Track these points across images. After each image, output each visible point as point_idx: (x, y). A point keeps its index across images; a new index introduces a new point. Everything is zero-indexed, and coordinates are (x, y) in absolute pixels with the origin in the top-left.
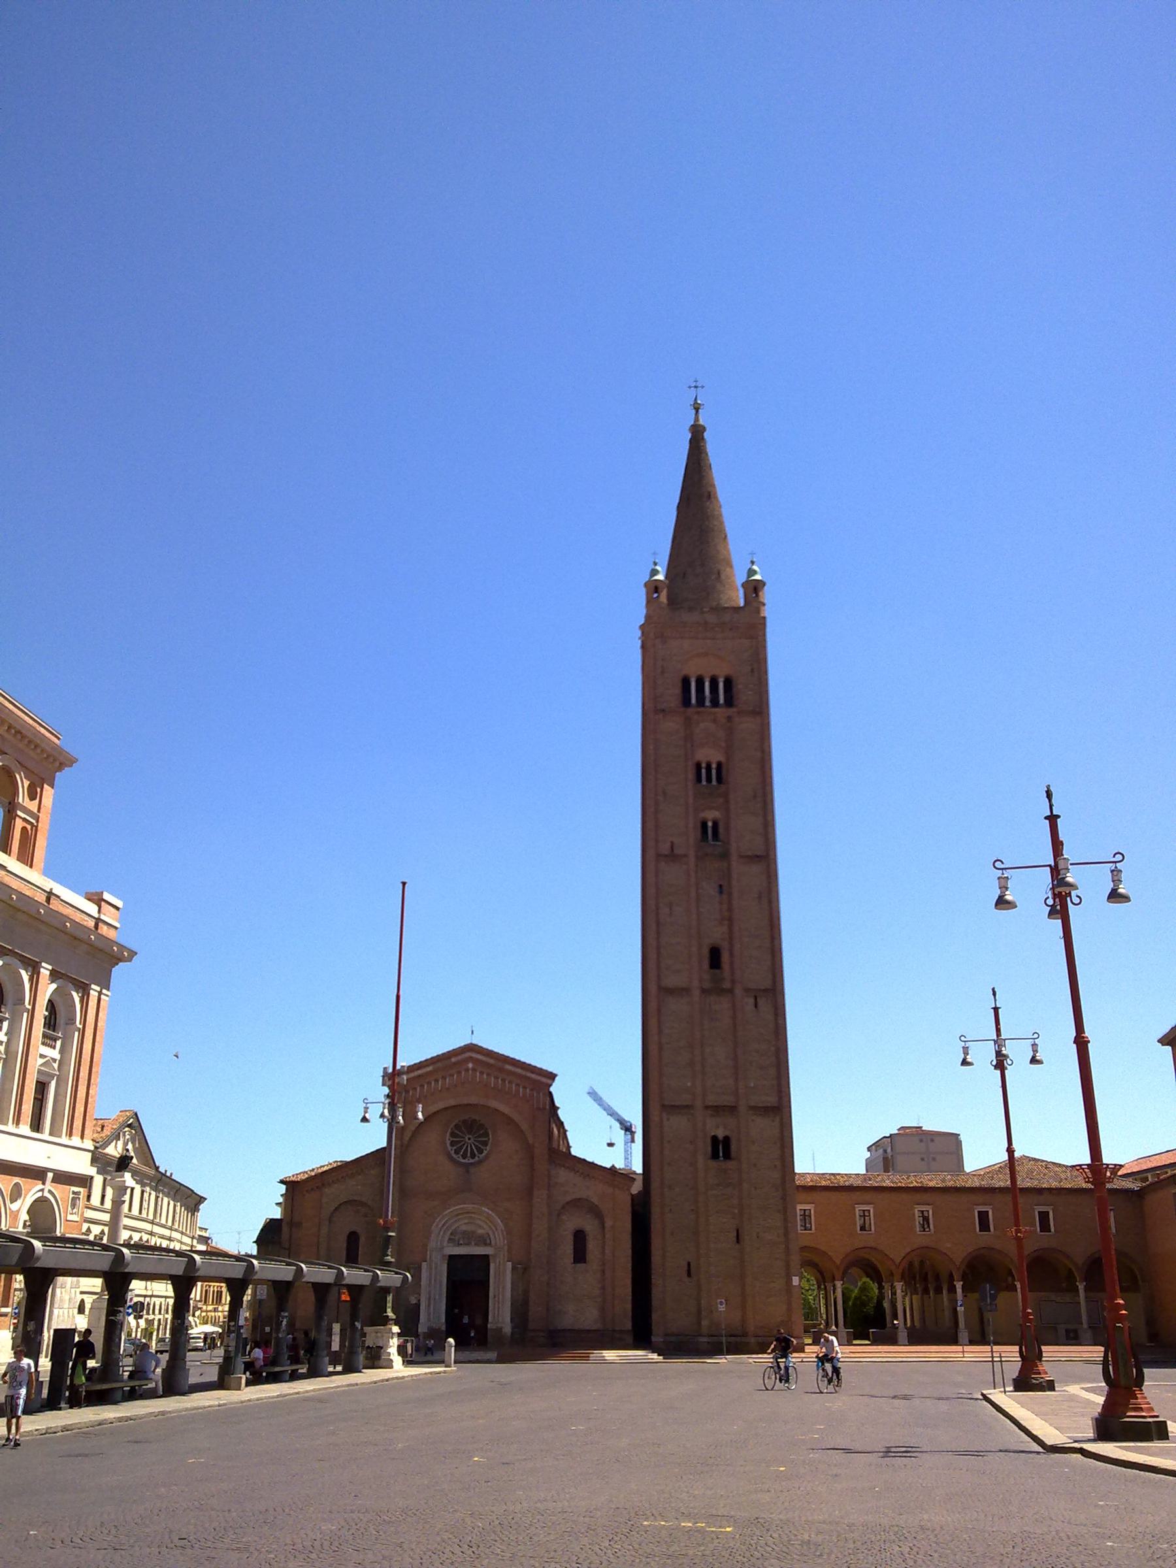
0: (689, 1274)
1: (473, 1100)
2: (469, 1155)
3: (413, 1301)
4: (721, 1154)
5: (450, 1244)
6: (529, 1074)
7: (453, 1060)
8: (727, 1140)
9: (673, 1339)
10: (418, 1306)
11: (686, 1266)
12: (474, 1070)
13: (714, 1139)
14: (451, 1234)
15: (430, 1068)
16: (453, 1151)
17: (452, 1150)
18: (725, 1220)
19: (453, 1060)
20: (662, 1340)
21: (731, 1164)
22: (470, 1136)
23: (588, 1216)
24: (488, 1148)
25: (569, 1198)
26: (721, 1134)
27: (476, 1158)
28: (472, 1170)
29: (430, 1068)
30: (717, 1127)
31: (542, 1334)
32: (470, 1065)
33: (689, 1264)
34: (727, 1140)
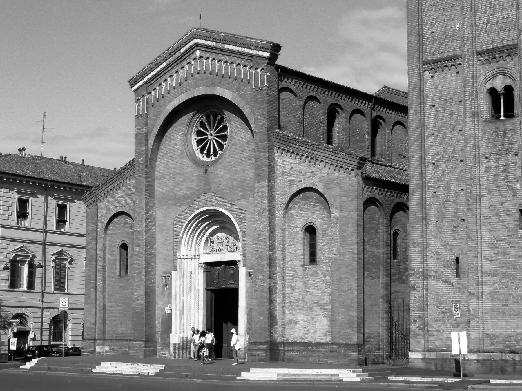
0: (458, 275)
1: (201, 91)
2: (212, 153)
3: (168, 312)
4: (502, 114)
5: (205, 251)
6: (247, 51)
7: (182, 51)
8: (509, 90)
9: (433, 355)
10: (170, 315)
11: (454, 262)
12: (201, 57)
13: (493, 92)
14: (207, 240)
15: (164, 64)
16: (199, 151)
17: (197, 149)
18: (504, 199)
19: (182, 51)
20: (421, 357)
21: (512, 124)
22: (212, 132)
23: (317, 208)
24: (227, 142)
25: (295, 189)
26: (499, 84)
27: (218, 155)
28: (210, 170)
29: (164, 64)
30: (494, 76)
31: (262, 347)
32: (198, 53)
33: (457, 259)
34: (509, 90)
